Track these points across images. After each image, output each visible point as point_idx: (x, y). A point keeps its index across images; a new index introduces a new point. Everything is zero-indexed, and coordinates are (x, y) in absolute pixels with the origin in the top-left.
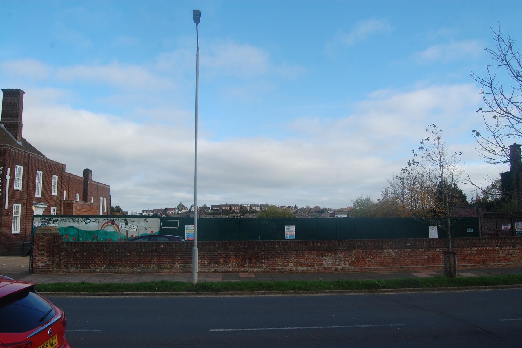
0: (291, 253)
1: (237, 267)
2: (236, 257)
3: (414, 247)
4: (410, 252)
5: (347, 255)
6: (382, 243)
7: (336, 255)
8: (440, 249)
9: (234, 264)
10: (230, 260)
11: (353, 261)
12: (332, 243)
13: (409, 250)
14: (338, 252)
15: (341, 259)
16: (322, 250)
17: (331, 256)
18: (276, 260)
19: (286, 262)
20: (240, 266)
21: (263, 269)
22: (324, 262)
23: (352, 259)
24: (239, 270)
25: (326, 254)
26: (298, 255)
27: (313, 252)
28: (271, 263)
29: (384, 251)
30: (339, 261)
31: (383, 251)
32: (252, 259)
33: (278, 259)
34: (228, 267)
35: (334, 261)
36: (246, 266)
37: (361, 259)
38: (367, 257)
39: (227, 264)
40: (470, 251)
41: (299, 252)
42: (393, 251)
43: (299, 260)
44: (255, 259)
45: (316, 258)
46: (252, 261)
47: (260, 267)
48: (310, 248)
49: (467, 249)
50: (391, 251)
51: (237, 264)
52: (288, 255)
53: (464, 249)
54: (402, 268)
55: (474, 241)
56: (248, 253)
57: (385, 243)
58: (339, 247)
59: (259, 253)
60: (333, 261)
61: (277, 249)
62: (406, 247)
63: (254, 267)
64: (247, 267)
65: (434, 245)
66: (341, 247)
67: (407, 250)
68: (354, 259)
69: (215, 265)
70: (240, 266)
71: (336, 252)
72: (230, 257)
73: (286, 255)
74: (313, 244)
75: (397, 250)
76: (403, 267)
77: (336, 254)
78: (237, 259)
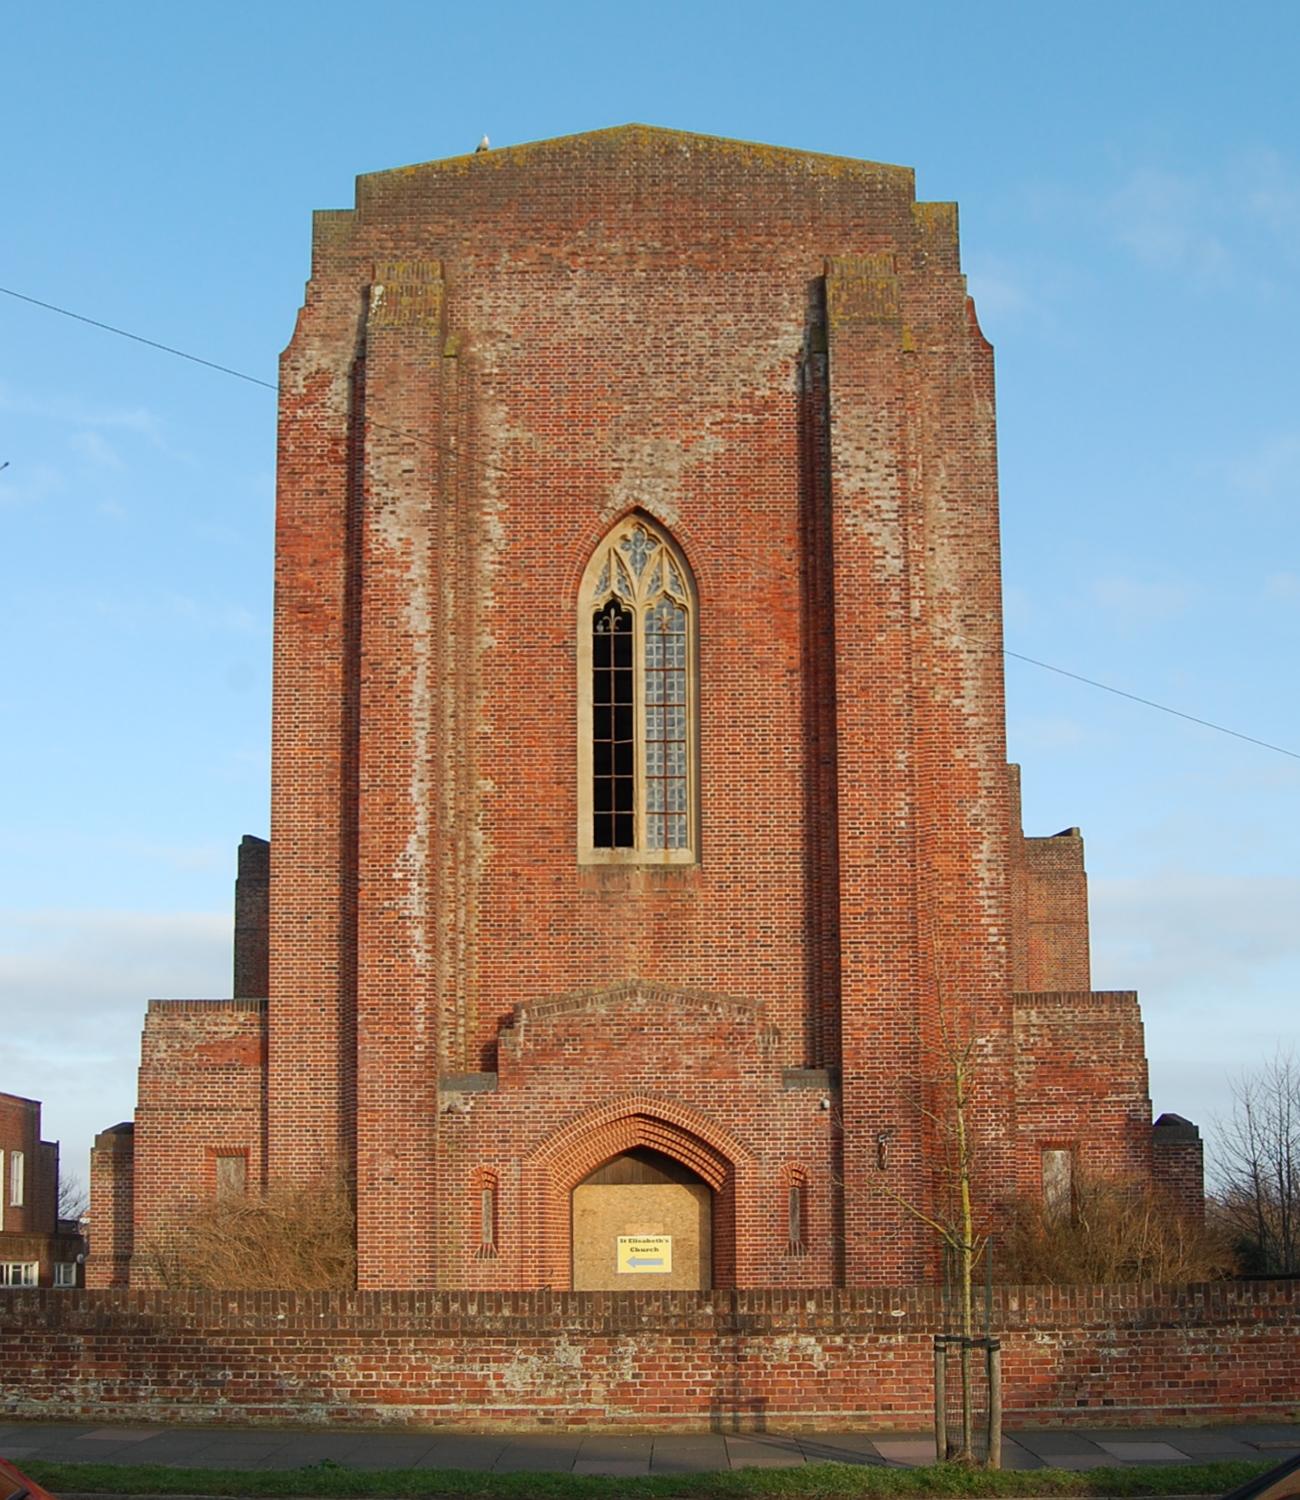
0: (340, 1343)
1: (102, 1399)
2: (99, 1358)
3: (926, 1323)
4: (904, 1348)
5: (598, 1357)
6: (769, 1305)
7: (546, 1358)
8: (1053, 1336)
9: (91, 1386)
10: (75, 1368)
11: (626, 1384)
12: (531, 1303)
13: (900, 1337)
14: (558, 1343)
15: (573, 1372)
16: (482, 1334)
17: (526, 1360)
18: (276, 1372)
19: (319, 1385)
20: (116, 1393)
21: (216, 1410)
22: (492, 1382)
23: (621, 1374)
24: (112, 1411)
25: (501, 1351)
26: (371, 1351)
27: (440, 1342)
28: (251, 1386)
29: (777, 1342)
30: (559, 1385)
31: (771, 1341)
32: (168, 1367)
33: (281, 1368)
34: (65, 1398)
35: (538, 1381)
36: (142, 1394)
37: (665, 1376)
38: (695, 1367)
39: (62, 1384)
40: (1204, 1342)
41: (381, 1343)
42: (819, 1340)
43: (379, 1376)
44: (181, 1367)
45: (458, 1365)
46: (169, 1378)
47: (205, 1400)
48: (428, 1324)
49: (1191, 1334)
50: (812, 1340)
51: (102, 1387)
52: (330, 1355)
53: (1175, 1334)
54: (861, 1418)
55: (1230, 1296)
56: (152, 1341)
57: (786, 1307)
58: (565, 1324)
59: (199, 1341)
60: (533, 1384)
61: (279, 1326)
62: (887, 1327)
63: (179, 1401)
64: (145, 1398)
65: (1023, 1317)
66: (573, 1324)
67: (889, 1339)
68: (635, 1376)
69: (12, 1388)
70: (116, 1393)
71: (551, 1343)
72: (73, 1357)
73: (318, 1351)
74: (446, 1308)
75: (838, 1340)
76: (863, 1413)
77: (549, 1351)
78: (104, 1366)
